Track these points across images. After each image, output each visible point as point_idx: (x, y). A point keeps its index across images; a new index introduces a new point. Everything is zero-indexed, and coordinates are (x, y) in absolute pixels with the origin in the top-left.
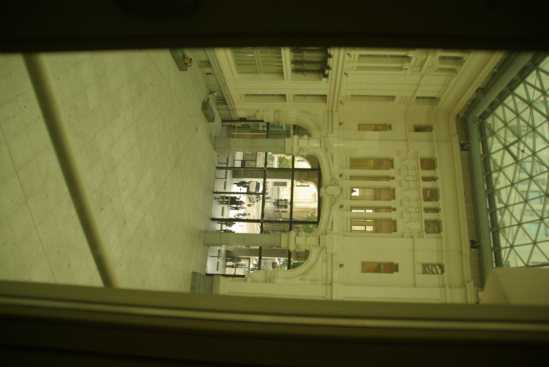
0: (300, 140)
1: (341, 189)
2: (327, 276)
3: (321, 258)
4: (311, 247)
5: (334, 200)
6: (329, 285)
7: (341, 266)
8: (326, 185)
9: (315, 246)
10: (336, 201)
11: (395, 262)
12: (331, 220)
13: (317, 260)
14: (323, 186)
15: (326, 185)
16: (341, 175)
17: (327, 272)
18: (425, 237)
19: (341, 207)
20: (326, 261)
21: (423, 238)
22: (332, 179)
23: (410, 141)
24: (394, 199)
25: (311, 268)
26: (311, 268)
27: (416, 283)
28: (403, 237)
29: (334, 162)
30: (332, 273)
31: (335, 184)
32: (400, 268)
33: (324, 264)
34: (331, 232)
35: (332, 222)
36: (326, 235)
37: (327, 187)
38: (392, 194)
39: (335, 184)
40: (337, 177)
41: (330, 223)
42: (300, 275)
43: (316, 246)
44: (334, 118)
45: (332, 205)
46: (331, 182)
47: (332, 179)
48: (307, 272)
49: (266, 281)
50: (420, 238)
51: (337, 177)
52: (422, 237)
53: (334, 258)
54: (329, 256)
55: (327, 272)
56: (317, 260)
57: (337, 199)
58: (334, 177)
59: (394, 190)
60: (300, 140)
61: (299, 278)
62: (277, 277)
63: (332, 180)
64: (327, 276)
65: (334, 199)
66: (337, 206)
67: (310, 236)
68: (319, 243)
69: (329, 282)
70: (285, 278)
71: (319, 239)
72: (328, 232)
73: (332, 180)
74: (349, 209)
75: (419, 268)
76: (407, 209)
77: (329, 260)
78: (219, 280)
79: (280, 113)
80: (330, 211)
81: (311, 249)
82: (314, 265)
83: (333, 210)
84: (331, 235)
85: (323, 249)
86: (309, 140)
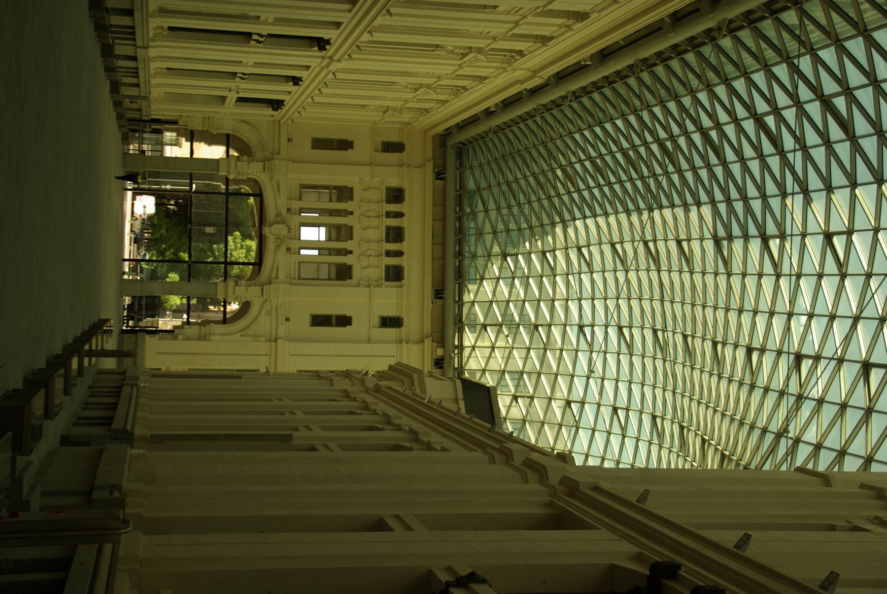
1: (289, 228)
3: (264, 311)
4: (253, 298)
7: (287, 319)
8: (271, 221)
9: (257, 296)
11: (348, 315)
12: (276, 266)
14: (267, 224)
16: (289, 210)
18: (383, 286)
19: (288, 249)
20: (269, 314)
22: (279, 214)
23: (375, 165)
24: (351, 239)
25: (253, 322)
26: (253, 322)
28: (358, 286)
30: (277, 327)
32: (354, 321)
34: (276, 280)
35: (277, 269)
37: (272, 225)
41: (275, 270)
43: (259, 297)
44: (281, 133)
45: (278, 247)
47: (279, 214)
49: (200, 337)
50: (378, 287)
54: (274, 308)
55: (271, 327)
59: (351, 227)
61: (239, 334)
62: (213, 334)
65: (280, 240)
66: (283, 249)
67: (252, 286)
68: (262, 293)
70: (223, 335)
71: (262, 289)
72: (273, 280)
74: (298, 211)
77: (274, 313)
78: (144, 339)
79: (211, 121)
80: (275, 255)
82: (256, 318)
84: (276, 284)
85: (266, 301)
86: (249, 162)
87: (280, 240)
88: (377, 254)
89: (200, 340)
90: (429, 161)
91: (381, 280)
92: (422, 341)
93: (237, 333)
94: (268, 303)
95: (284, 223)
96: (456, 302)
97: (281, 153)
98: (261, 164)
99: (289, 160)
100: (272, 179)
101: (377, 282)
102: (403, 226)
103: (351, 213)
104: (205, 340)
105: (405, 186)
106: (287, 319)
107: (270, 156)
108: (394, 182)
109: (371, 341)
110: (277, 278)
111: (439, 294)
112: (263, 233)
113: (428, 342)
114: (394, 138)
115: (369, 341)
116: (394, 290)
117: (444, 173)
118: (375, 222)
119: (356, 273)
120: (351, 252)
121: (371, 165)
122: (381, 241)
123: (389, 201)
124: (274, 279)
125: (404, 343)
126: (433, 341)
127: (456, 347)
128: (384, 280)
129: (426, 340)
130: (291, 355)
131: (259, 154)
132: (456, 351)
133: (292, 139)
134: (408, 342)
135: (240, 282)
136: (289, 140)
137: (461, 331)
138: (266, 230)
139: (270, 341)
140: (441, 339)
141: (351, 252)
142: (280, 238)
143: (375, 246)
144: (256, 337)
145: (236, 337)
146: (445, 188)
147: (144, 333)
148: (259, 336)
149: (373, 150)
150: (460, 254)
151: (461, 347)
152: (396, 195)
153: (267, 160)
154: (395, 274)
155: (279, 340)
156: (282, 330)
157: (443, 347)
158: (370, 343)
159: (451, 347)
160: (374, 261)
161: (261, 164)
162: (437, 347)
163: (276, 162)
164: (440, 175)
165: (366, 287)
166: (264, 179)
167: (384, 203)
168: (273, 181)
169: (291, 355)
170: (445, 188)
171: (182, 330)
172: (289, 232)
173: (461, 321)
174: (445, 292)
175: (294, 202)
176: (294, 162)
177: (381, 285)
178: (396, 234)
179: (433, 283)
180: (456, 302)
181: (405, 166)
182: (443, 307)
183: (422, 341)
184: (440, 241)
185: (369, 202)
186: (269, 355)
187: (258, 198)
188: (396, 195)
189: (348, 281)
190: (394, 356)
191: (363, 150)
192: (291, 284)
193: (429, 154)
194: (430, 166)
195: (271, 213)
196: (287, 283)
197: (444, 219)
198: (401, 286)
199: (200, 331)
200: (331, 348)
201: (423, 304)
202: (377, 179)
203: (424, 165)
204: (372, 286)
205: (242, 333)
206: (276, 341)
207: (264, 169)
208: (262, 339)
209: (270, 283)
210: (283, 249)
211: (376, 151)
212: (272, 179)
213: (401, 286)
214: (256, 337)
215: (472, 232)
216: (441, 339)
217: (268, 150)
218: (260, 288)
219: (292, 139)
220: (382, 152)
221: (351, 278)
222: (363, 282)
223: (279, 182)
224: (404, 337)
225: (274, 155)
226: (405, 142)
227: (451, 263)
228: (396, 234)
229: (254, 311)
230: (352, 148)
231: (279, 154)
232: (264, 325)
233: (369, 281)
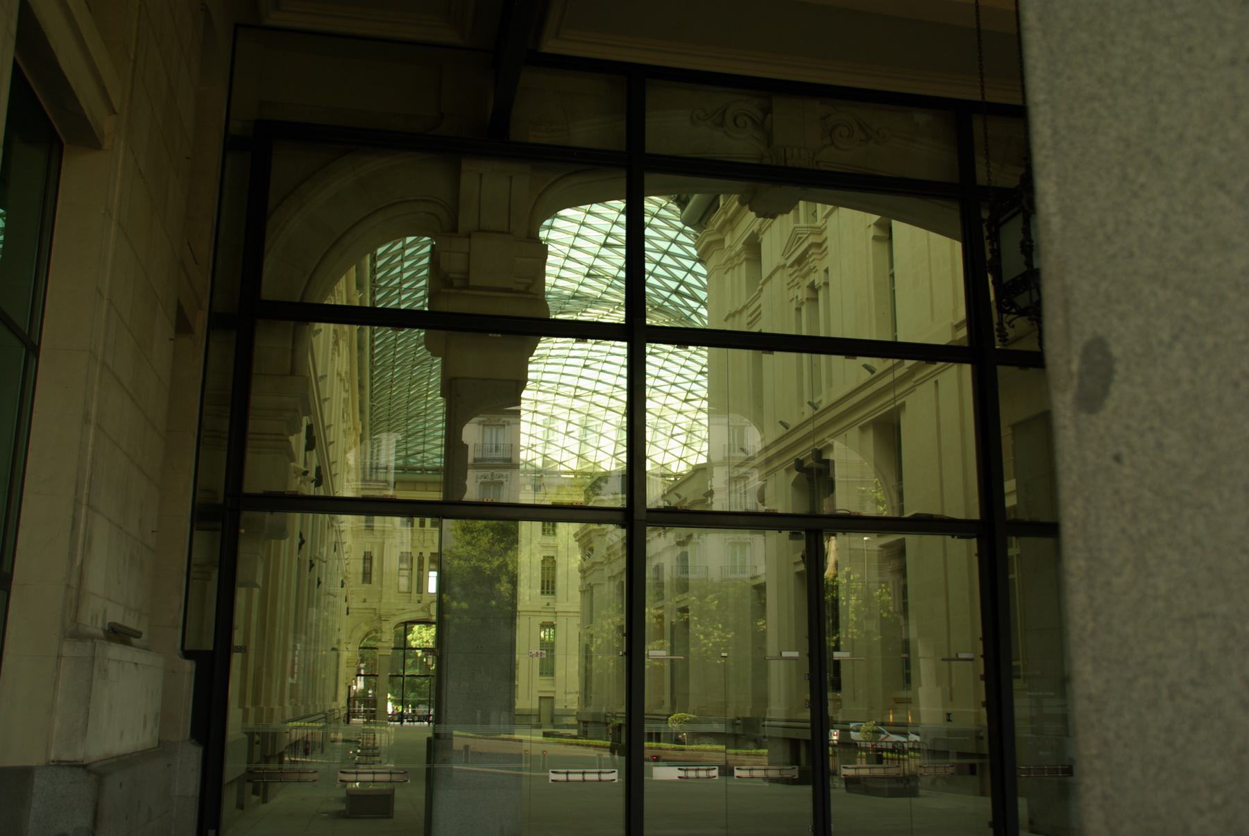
16: (419, 602)
22: (422, 610)
40: (420, 606)
47: (422, 610)
51: (420, 606)
95: (429, 605)
97: (374, 607)
168: (396, 613)
231: (375, 609)
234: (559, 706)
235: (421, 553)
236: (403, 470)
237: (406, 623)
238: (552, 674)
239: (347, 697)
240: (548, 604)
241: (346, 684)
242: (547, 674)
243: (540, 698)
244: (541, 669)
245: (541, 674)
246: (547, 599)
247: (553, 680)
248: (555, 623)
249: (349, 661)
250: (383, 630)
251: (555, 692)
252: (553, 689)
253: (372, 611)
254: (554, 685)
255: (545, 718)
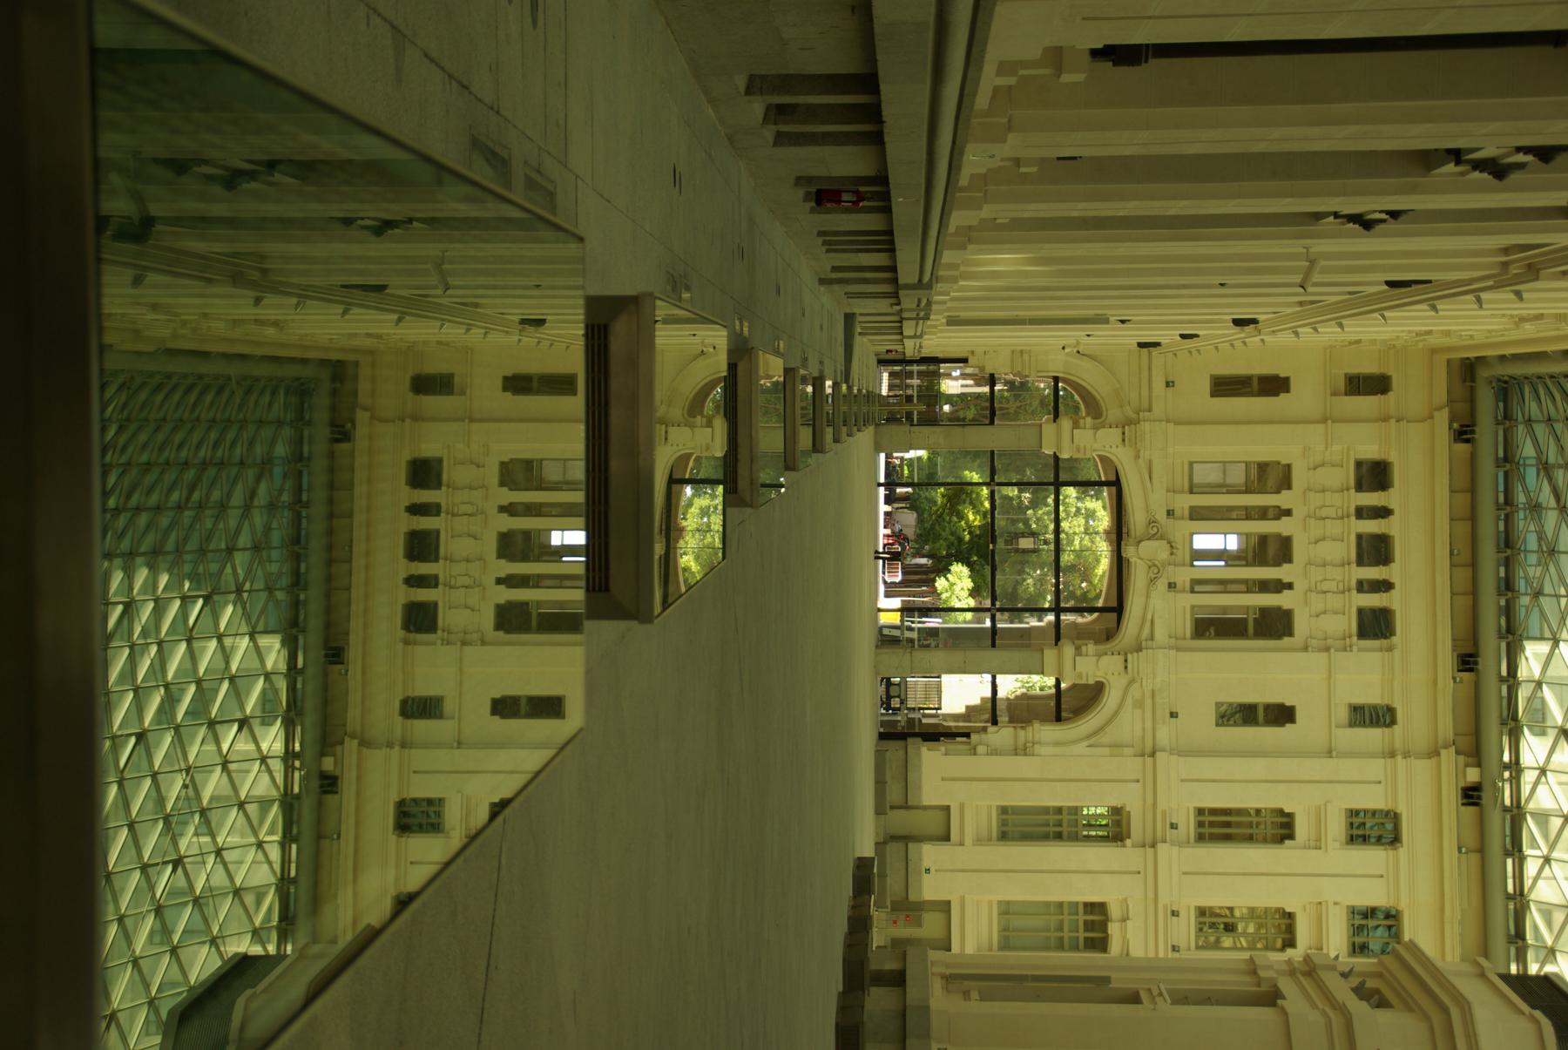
0: (1075, 431)
1: (1172, 547)
2: (1143, 737)
3: (1129, 700)
5: (1156, 571)
6: (1149, 847)
7: (1173, 715)
8: (1138, 534)
9: (1116, 673)
10: (1160, 574)
12: (1149, 617)
13: (1121, 705)
15: (1138, 534)
16: (1170, 513)
17: (1144, 729)
18: (1355, 648)
19: (1172, 586)
20: (1139, 704)
21: (1351, 651)
22: (1152, 522)
23: (1333, 422)
24: (1290, 561)
27: (1333, 745)
28: (1306, 649)
29: (1155, 476)
31: (1158, 531)
32: (1299, 715)
33: (1138, 712)
34: (1149, 643)
36: (1140, 653)
37: (1140, 542)
38: (1282, 550)
39: (1158, 531)
40: (1161, 516)
41: (1148, 624)
42: (1089, 737)
43: (1120, 674)
45: (1152, 581)
46: (1147, 527)
47: (1152, 522)
48: (1101, 729)
51: (1161, 516)
52: (1348, 649)
53: (1158, 700)
54: (1148, 694)
55: (1144, 729)
56: (1121, 705)
57: (1161, 569)
58: (1153, 516)
60: (1075, 431)
61: (1086, 743)
62: (1039, 743)
63: (1150, 524)
64: (1143, 737)
66: (1162, 585)
67: (1106, 654)
68: (1126, 667)
69: (1148, 749)
70: (1057, 744)
71: (1126, 661)
72: (1144, 643)
73: (1150, 524)
75: (1343, 714)
76: (1318, 584)
77: (1148, 702)
78: (919, 749)
80: (1148, 596)
81: (1109, 684)
82: (1116, 714)
83: (1153, 594)
84: (1150, 651)
85: (1133, 681)
86: (1096, 428)
87: (1155, 569)
88: (1341, 587)
89: (1016, 754)
90: (1439, 409)
91: (1350, 637)
92: (1434, 753)
93: (1082, 739)
94: (1136, 685)
95: (1162, 538)
96: (1502, 680)
98: (1115, 433)
99: (1168, 421)
100: (1137, 457)
101: (1342, 642)
102: (1392, 534)
103: (1288, 513)
104: (1025, 755)
105: (1393, 457)
106: (1173, 715)
107: (1133, 416)
108: (1371, 452)
109: (1334, 753)
110: (1152, 638)
111: (1467, 661)
112: (1124, 555)
113: (1448, 756)
114: (1369, 368)
115: (1329, 753)
116: (1376, 656)
117: (1473, 432)
118: (1334, 528)
119: (1301, 625)
120: (1290, 586)
121: (1324, 420)
122: (1344, 564)
123: (1359, 487)
124: (1146, 640)
125: (1399, 758)
126: (1458, 753)
127: (1506, 767)
128: (1355, 638)
129: (1443, 752)
130: (1182, 781)
131: (1113, 413)
132: (1507, 774)
133: (1173, 382)
134: (1406, 755)
135: (1084, 648)
136: (1168, 384)
137: (1515, 736)
138: (1129, 552)
139: (1143, 755)
140: (1474, 752)
141: (1290, 586)
142: (1155, 565)
143: (1336, 573)
144: (1116, 747)
145: (1081, 748)
146: (1473, 459)
147: (919, 740)
148: (1121, 746)
149: (1328, 392)
150: (1507, 586)
151: (1516, 767)
152: (1375, 475)
153: (1126, 423)
154: (1375, 625)
155: (1158, 754)
156: (1165, 734)
157: (1479, 765)
158: (1331, 757)
159: (1493, 766)
160: (1334, 601)
161: (1115, 433)
162: (1467, 765)
163: (1146, 426)
164: (1464, 433)
165: (1320, 650)
166: (1123, 458)
167: (1353, 491)
168: (1141, 460)
169: (1182, 781)
170: (1473, 459)
171: (983, 736)
172: (1172, 554)
173: (1515, 718)
174: (1480, 660)
175: (1177, 496)
176: (1176, 423)
177: (1351, 646)
178: (1376, 550)
179: (1454, 640)
180: (1502, 680)
181: (1393, 421)
182: (1477, 688)
183: (1434, 753)
184: (1466, 560)
185: (1323, 491)
186: (1141, 781)
187: (1114, 489)
188: (1375, 475)
189: (1286, 639)
190: (1380, 782)
191: (1305, 396)
192: (1178, 649)
193: (1441, 395)
194: (1443, 418)
195: (1137, 518)
196: (1170, 648)
197: (1473, 518)
198: (1390, 649)
199: (1016, 737)
200: (1257, 768)
201: (1435, 682)
202: (1336, 448)
203: (1431, 417)
204: (1332, 650)
205: (1092, 741)
206: (1153, 755)
207: (1124, 440)
208: (1127, 751)
209: (1139, 649)
210: (1162, 585)
211: (1334, 394)
212: (1137, 457)
213: (1390, 649)
214: (1116, 747)
215: (1532, 542)
216: (1474, 752)
217: (1129, 403)
218: (1121, 658)
219: (1173, 382)
220: (1346, 395)
221: (1290, 634)
222: (1314, 642)
223: (1150, 462)
224: (1398, 745)
225: (1141, 414)
226: (1390, 373)
227: (1490, 603)
228: (1376, 550)
229: (1111, 699)
230: (1288, 391)
231: (1150, 410)
232: (1130, 725)
233: (1326, 639)
234: (930, 854)
235: (1288, 513)
236: (1506, 459)
237: (1116, 484)
238: (1004, 837)
239: (940, 355)
240: (1173, 826)
241: (973, 353)
242: (1004, 823)
243: (948, 808)
244: (1017, 811)
245: (1004, 810)
246: (1188, 825)
247: (990, 839)
248: (1128, 842)
249: (1026, 357)
250: (1101, 432)
251: (961, 844)
252: (968, 840)
253: (1145, 405)
254: (978, 841)
255: (899, 821)
